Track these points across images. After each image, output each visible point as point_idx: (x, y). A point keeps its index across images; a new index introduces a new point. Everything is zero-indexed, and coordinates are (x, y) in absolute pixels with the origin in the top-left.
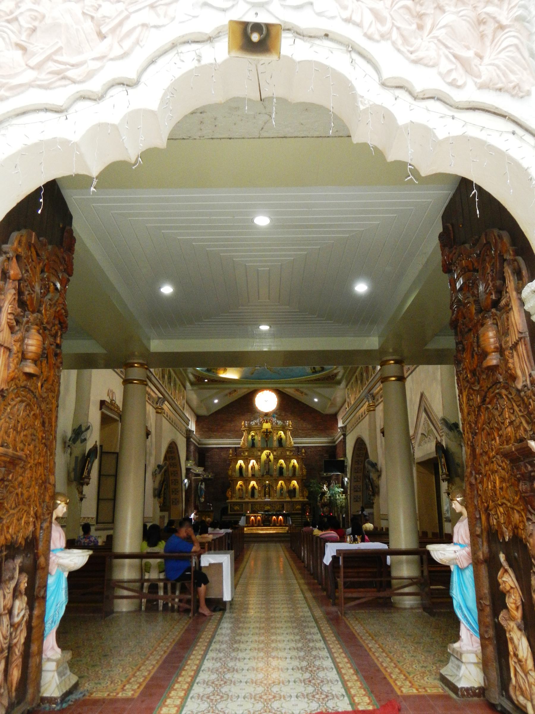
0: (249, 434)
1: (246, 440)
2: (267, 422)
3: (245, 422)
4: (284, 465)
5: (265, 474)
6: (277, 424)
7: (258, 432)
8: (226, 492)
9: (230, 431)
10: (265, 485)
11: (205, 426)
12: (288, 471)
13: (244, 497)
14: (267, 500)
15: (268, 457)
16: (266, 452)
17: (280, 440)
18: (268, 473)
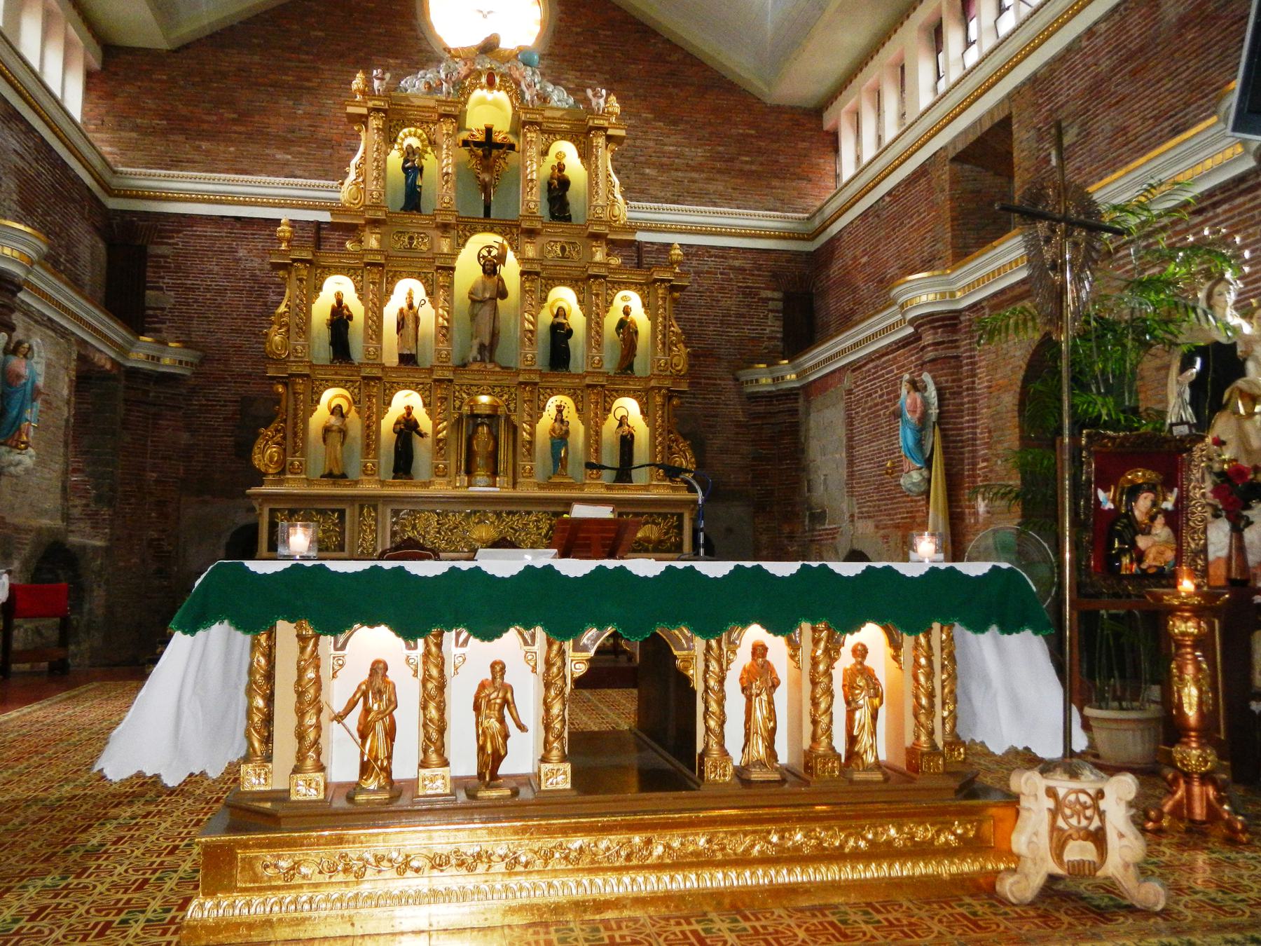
0: (390, 138)
1: (371, 167)
2: (491, 84)
3: (368, 82)
4: (577, 319)
5: (474, 352)
6: (544, 98)
7: (447, 127)
8: (250, 450)
9: (285, 143)
10: (474, 416)
11: (150, 103)
12: (599, 344)
13: (354, 472)
14: (481, 488)
15: (491, 267)
16: (480, 241)
17: (558, 188)
18: (488, 350)
